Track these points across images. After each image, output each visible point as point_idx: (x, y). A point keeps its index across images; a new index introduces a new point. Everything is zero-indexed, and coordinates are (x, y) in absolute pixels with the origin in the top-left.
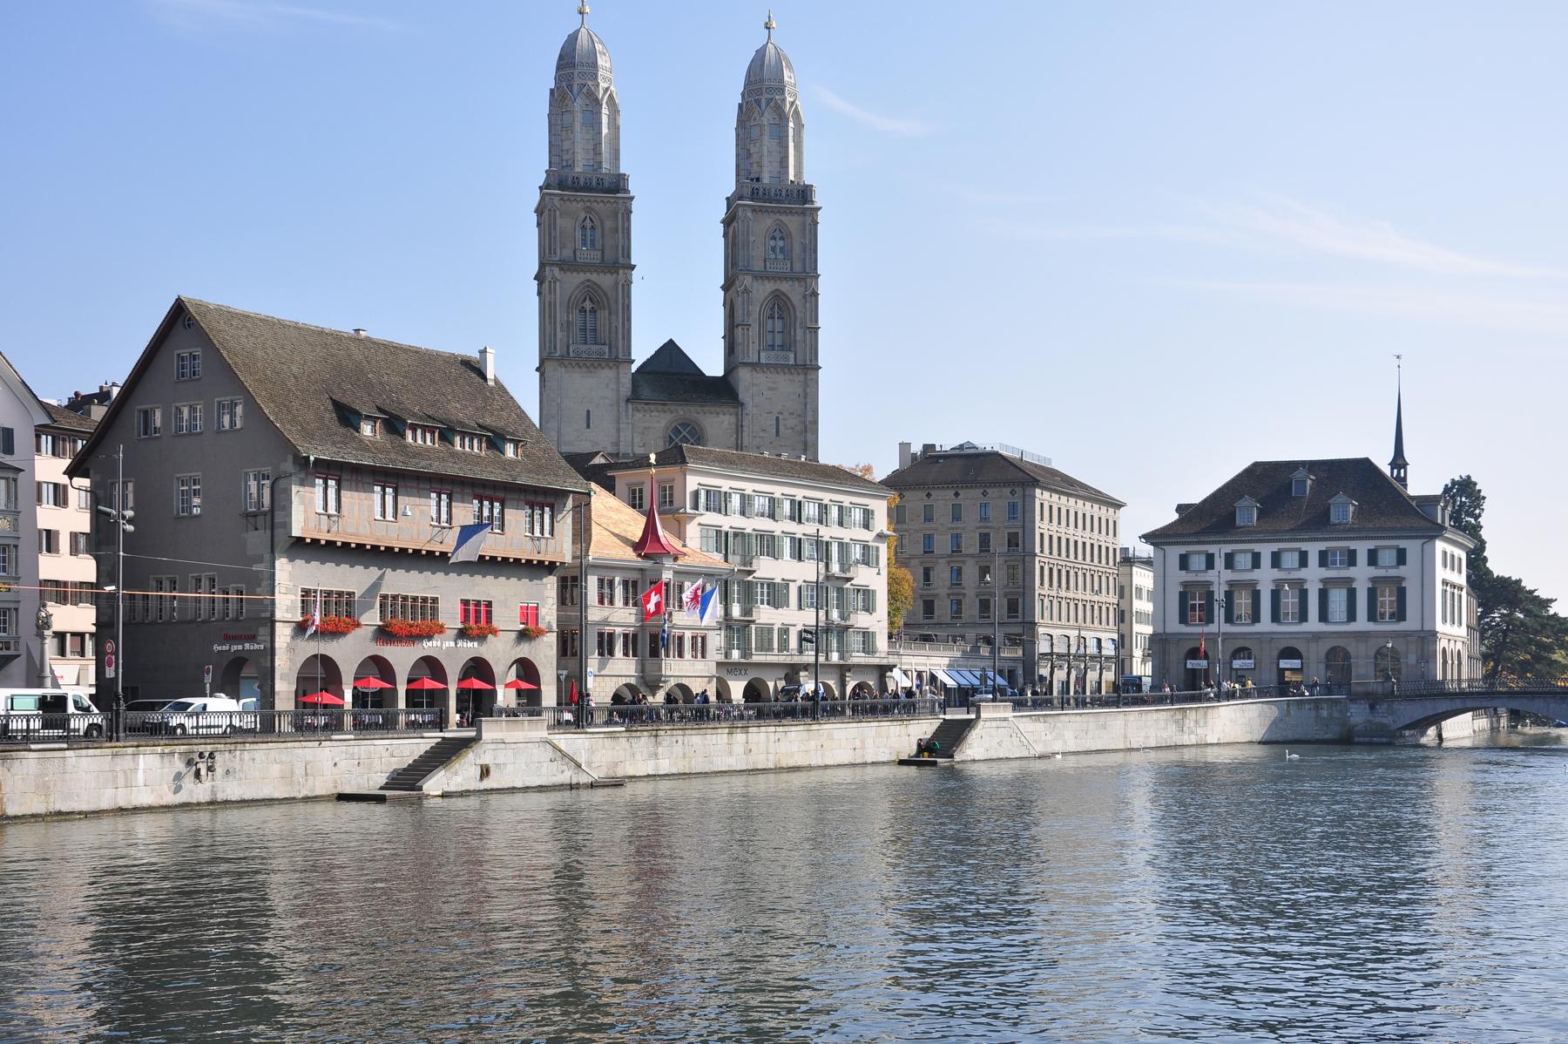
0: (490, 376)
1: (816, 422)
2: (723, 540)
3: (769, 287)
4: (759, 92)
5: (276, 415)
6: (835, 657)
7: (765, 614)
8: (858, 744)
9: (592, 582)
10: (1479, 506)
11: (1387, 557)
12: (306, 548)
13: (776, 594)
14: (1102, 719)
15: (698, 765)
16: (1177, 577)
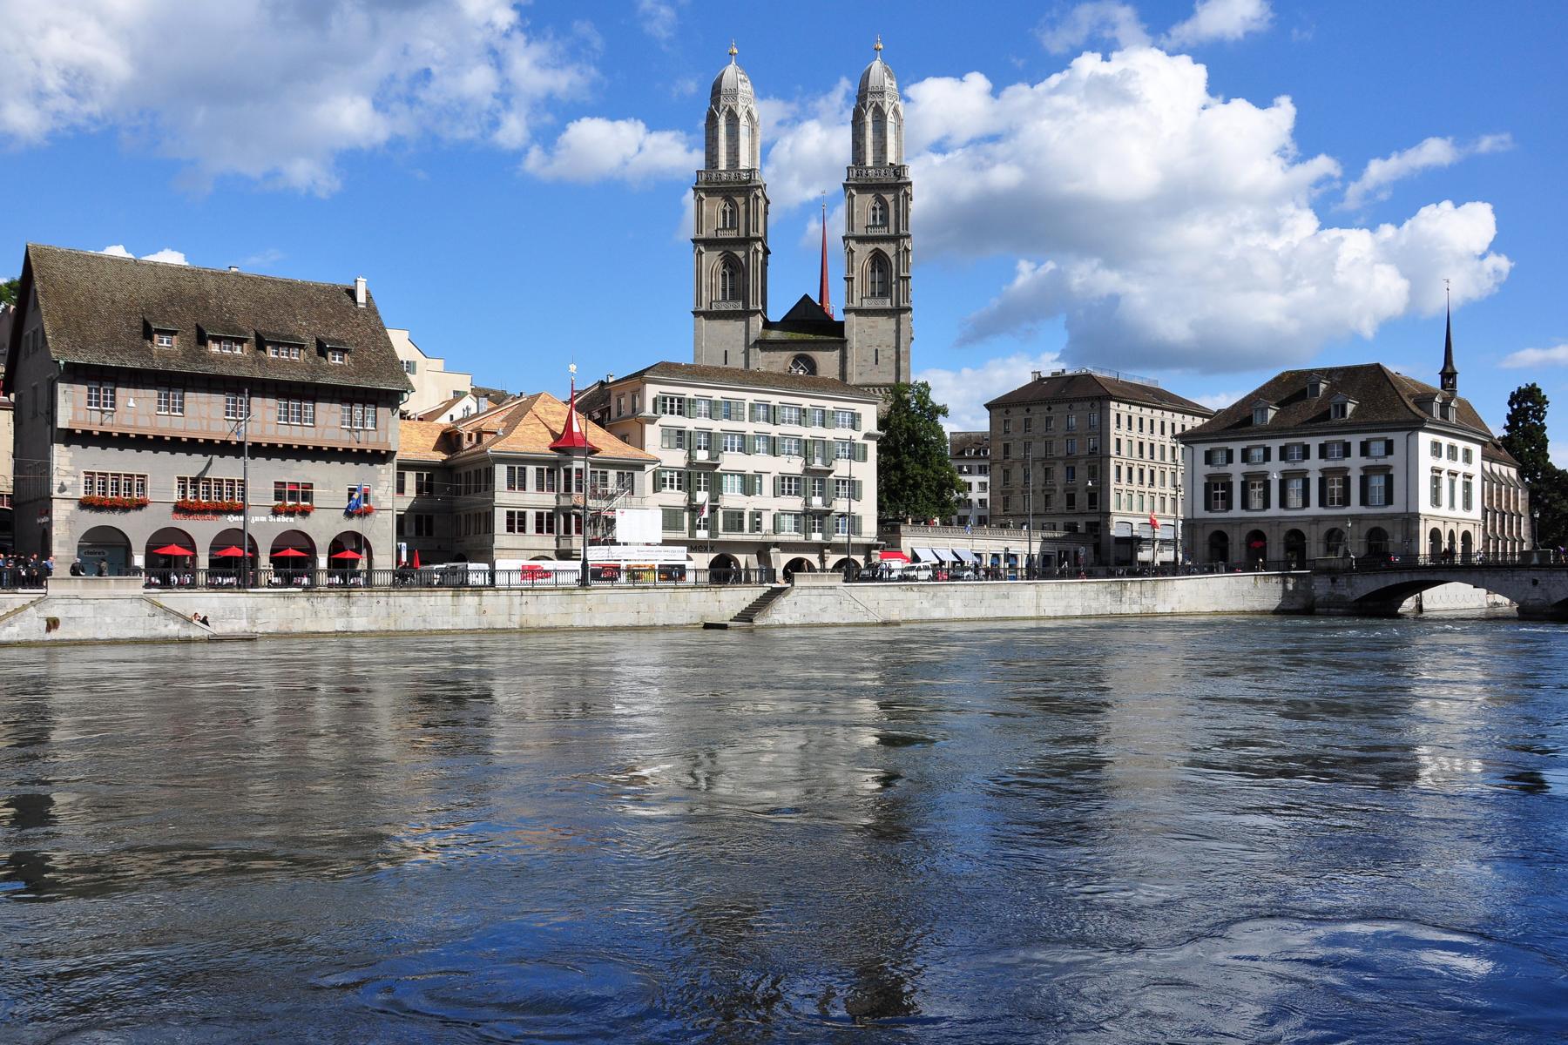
0: (361, 298)
1: (908, 352)
2: (681, 438)
3: (870, 247)
4: (865, 97)
5: (58, 332)
6: (817, 537)
7: (732, 498)
8: (643, 607)
9: (501, 472)
10: (1542, 410)
11: (1377, 448)
12: (70, 437)
13: (749, 484)
14: (1004, 590)
15: (407, 624)
16: (1203, 470)
